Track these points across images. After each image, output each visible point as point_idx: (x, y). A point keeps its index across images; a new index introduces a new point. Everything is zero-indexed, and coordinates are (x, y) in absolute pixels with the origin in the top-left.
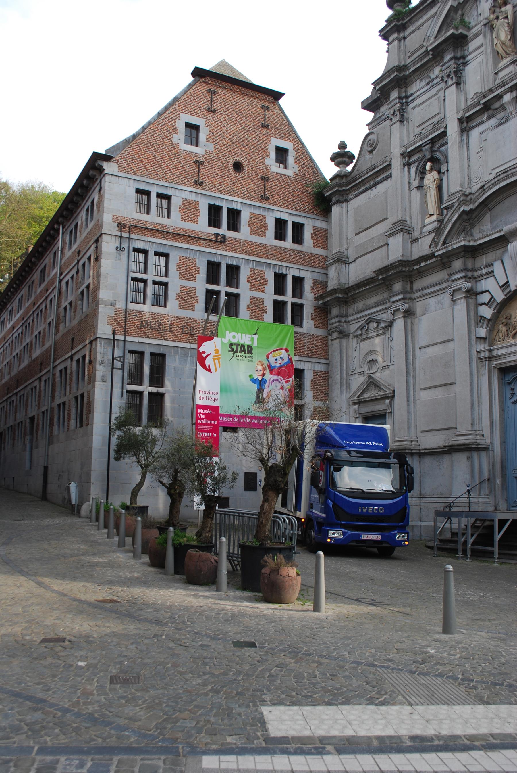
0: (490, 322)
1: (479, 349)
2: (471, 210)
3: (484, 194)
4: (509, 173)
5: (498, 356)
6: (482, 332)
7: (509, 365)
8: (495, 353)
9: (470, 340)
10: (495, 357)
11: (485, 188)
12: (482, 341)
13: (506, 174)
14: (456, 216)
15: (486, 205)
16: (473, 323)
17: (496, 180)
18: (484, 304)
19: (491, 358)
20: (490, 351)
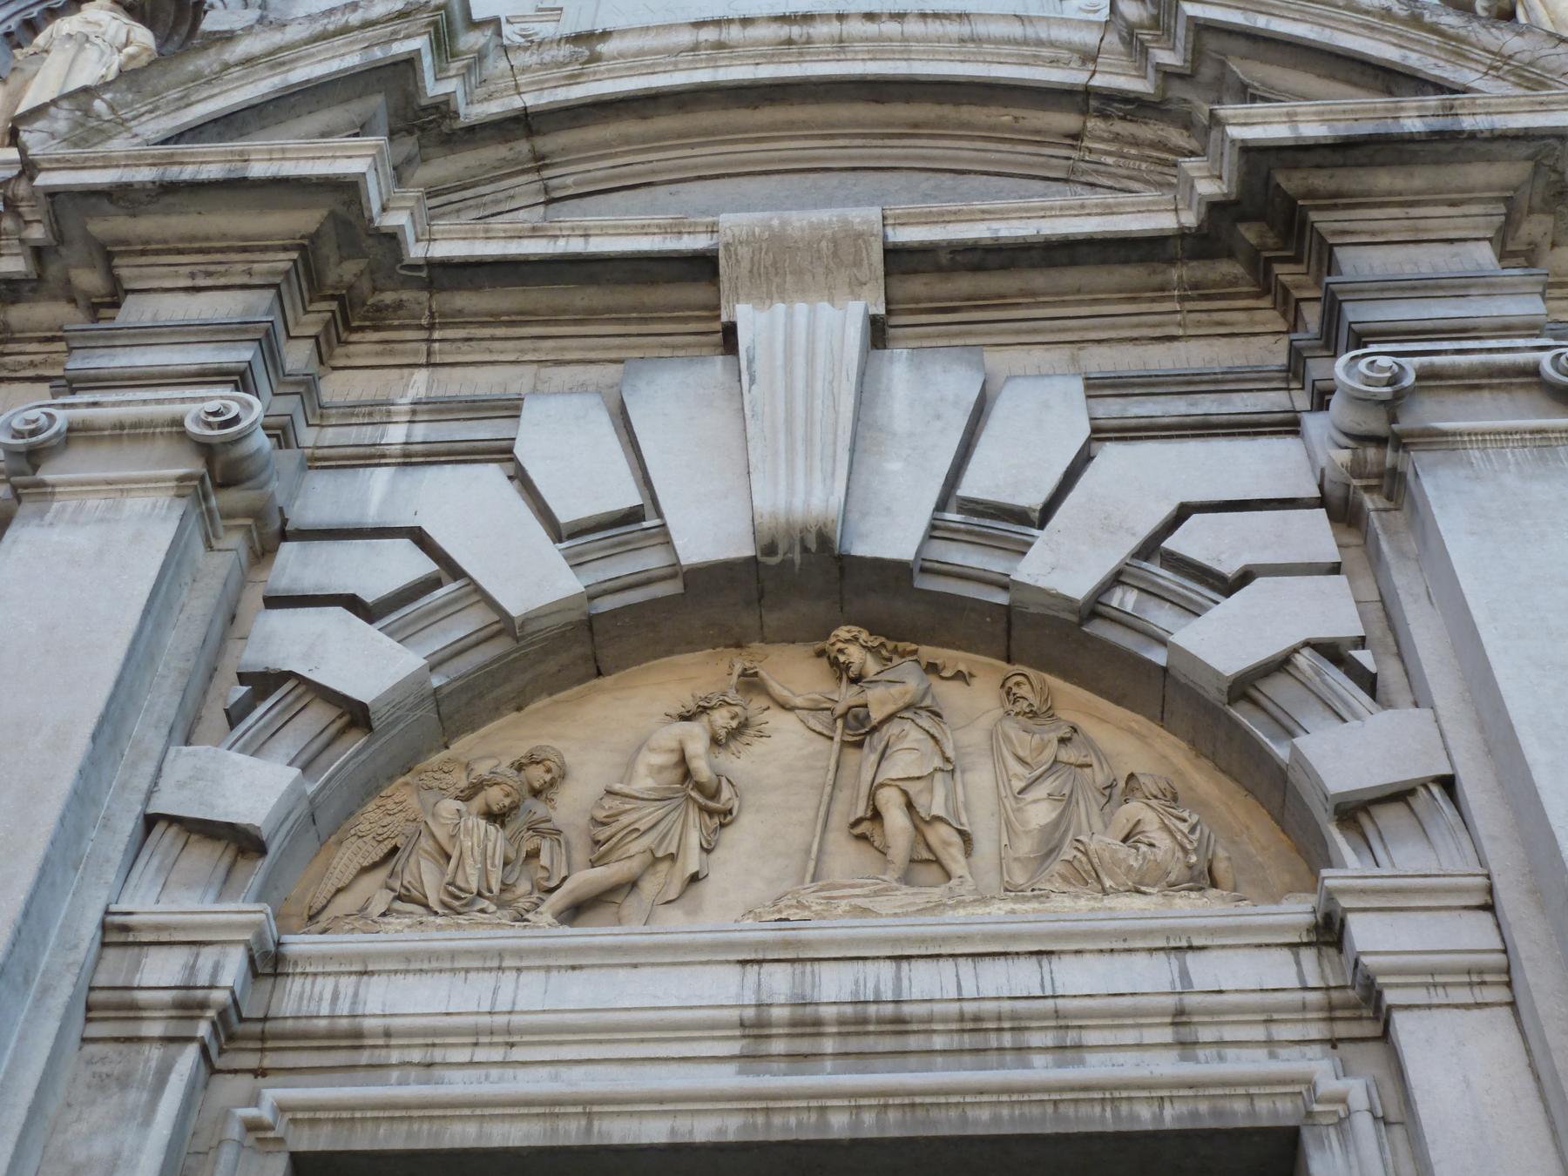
0: (355, 743)
1: (145, 903)
2: (444, 109)
3: (573, 79)
4: (821, 30)
5: (355, 1038)
6: (251, 784)
7: (462, 1135)
8: (304, 999)
9: (83, 797)
10: (302, 1038)
11: (602, 48)
12: (205, 857)
13: (795, 31)
14: (352, 60)
15: (540, 162)
16: (161, 700)
17: (708, 34)
18: (352, 603)
19: (234, 1036)
20: (268, 964)
